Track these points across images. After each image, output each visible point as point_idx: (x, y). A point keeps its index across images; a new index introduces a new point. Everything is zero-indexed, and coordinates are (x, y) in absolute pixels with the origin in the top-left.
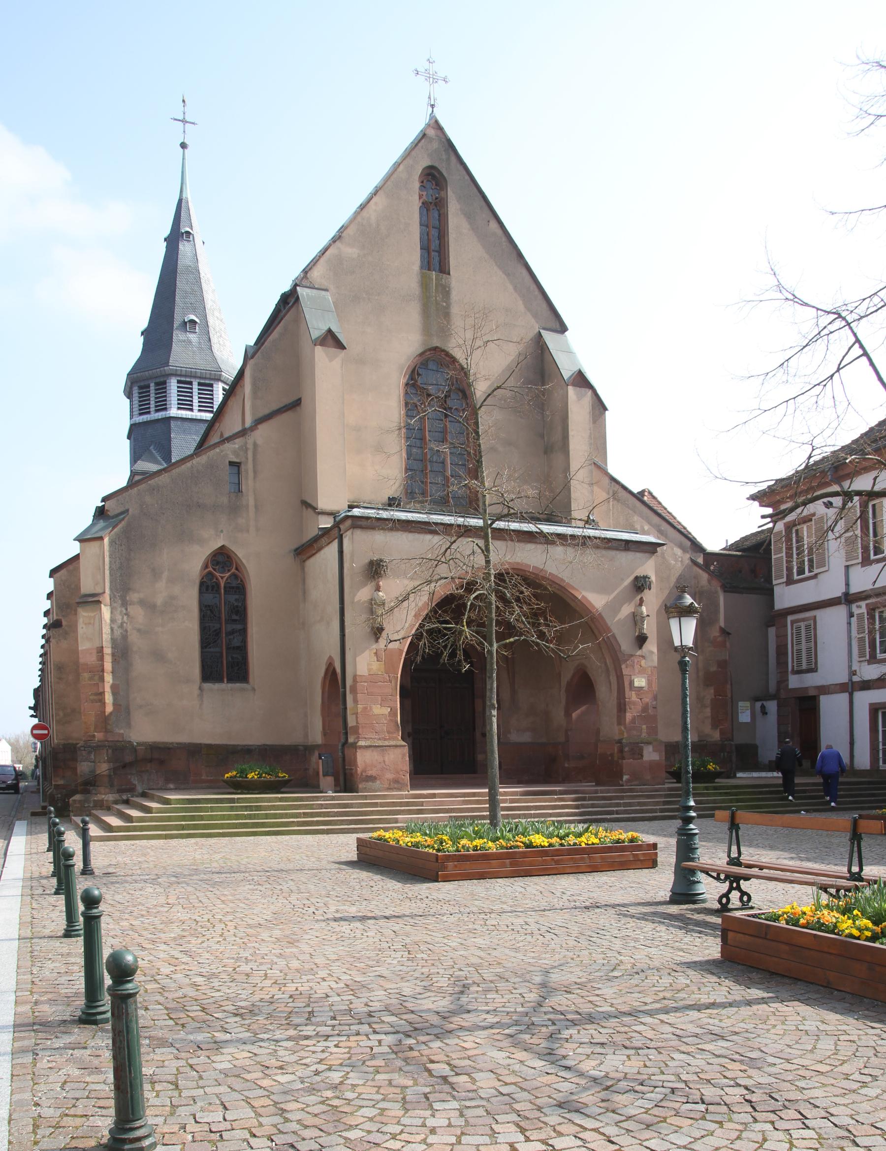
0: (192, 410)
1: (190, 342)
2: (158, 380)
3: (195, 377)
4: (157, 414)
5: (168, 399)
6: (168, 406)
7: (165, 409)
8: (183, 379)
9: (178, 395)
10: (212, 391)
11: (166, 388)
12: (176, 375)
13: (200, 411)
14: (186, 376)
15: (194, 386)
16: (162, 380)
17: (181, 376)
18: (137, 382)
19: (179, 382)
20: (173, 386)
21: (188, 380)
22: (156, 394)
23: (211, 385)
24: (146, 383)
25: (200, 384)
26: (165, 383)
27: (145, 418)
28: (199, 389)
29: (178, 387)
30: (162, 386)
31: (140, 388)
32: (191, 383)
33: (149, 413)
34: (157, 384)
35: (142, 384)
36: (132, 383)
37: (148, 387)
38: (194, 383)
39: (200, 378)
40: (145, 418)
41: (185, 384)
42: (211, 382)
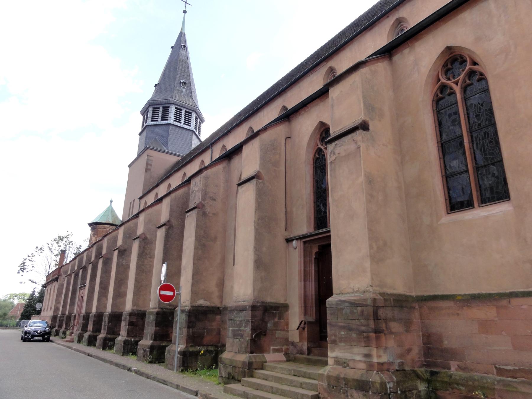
0: (180, 123)
1: (182, 92)
2: (165, 106)
3: (184, 107)
4: (162, 122)
5: (169, 117)
6: (169, 119)
7: (167, 120)
8: (178, 107)
9: (175, 114)
10: (191, 116)
11: (169, 110)
12: (175, 104)
13: (184, 124)
14: (180, 106)
15: (183, 112)
16: (167, 105)
17: (177, 105)
18: (152, 105)
19: (176, 108)
20: (172, 110)
21: (180, 108)
22: (163, 112)
23: (191, 113)
24: (158, 106)
25: (186, 111)
26: (168, 107)
27: (155, 123)
28: (185, 114)
29: (175, 111)
30: (166, 109)
31: (154, 108)
32: (181, 110)
33: (157, 121)
34: (164, 107)
35: (155, 106)
36: (150, 106)
37: (159, 108)
38: (183, 110)
39: (186, 108)
40: (155, 123)
41: (178, 111)
42: (191, 112)
